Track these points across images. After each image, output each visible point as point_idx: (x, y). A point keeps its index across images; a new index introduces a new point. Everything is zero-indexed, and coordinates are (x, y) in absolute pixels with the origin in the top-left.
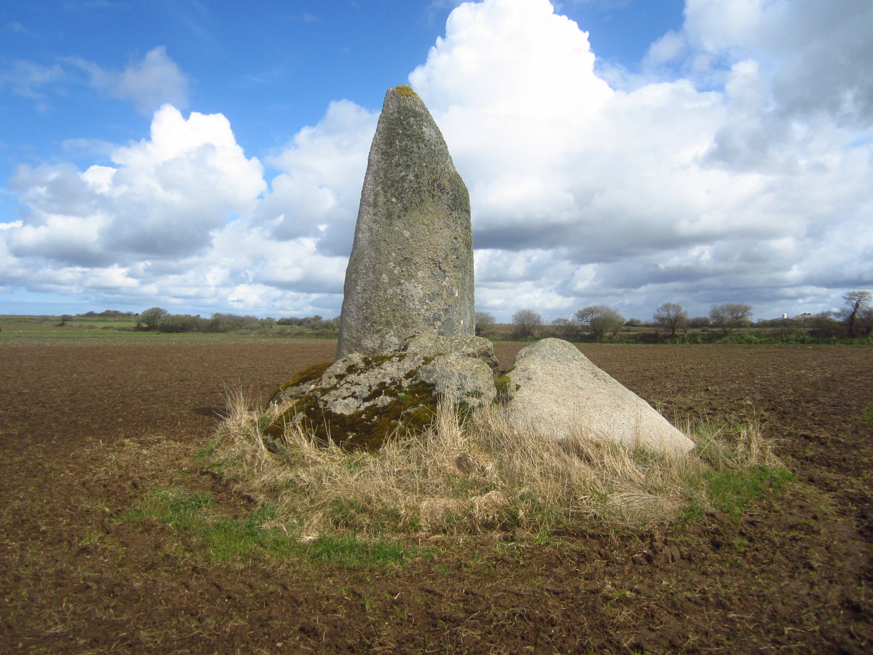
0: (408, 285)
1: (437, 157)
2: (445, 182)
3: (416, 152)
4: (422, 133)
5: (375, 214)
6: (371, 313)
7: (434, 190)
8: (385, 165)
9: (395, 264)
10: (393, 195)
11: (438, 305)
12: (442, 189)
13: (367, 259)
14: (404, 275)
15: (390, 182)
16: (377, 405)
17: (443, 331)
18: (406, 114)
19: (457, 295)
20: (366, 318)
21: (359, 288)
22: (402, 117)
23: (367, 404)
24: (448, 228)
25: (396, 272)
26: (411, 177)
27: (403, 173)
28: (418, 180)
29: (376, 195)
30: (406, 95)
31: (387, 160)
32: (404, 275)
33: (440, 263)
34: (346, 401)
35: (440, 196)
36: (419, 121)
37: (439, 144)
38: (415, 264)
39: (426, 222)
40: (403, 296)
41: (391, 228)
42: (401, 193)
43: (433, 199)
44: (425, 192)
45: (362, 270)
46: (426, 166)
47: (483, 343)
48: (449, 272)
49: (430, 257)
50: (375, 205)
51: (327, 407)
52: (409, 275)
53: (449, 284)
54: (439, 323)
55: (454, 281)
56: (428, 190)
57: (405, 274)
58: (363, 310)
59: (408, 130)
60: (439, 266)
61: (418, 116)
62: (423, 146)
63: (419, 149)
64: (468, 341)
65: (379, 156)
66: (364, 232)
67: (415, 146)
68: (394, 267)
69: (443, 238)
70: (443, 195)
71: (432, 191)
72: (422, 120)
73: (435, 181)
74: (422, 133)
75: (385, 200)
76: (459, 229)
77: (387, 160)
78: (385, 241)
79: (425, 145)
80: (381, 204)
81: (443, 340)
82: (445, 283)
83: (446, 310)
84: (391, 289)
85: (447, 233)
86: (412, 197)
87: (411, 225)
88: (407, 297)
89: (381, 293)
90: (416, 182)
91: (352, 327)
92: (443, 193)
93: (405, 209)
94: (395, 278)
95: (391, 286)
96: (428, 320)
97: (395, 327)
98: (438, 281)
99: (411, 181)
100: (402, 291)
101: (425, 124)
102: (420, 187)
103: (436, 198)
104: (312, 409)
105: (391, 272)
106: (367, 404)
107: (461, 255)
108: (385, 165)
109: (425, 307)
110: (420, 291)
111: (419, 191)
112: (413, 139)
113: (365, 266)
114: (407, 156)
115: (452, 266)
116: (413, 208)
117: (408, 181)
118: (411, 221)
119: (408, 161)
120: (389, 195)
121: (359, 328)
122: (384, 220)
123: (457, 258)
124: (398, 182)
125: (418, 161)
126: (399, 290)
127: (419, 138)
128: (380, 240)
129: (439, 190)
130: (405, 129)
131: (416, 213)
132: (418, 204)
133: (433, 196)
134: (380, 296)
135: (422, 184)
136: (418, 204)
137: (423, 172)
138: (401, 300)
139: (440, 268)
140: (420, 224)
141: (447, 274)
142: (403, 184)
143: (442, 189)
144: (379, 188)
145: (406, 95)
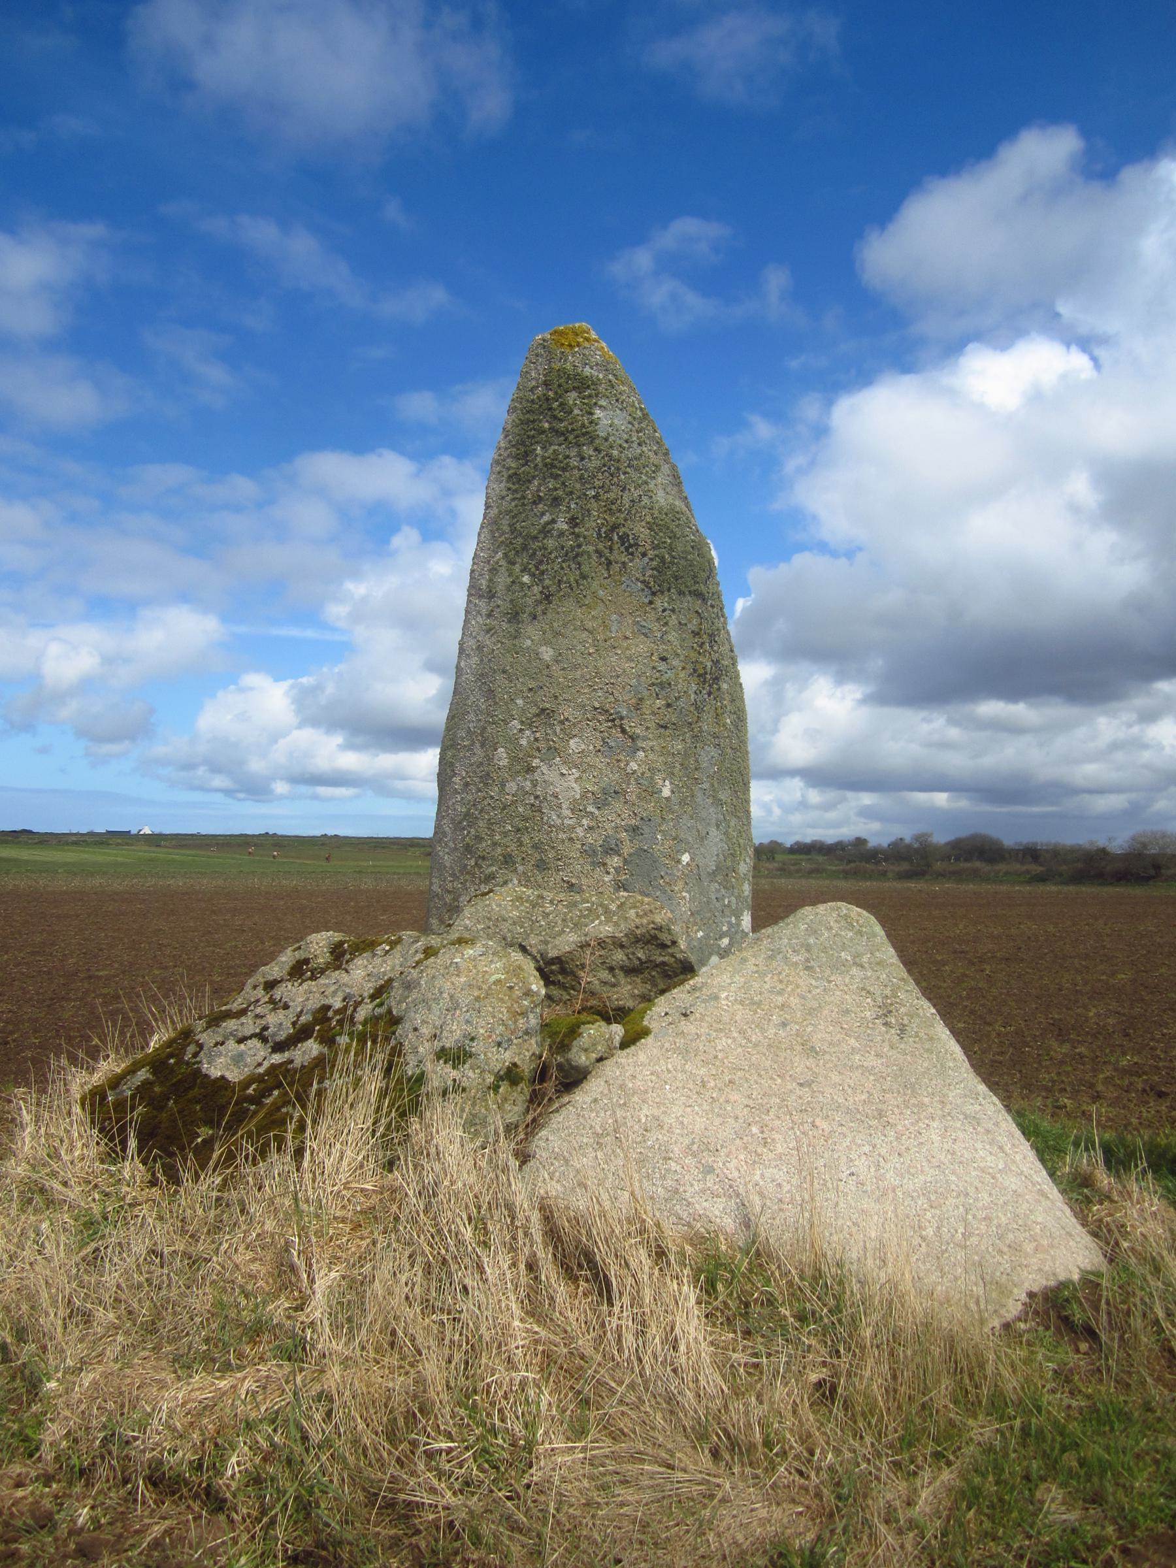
0: (546, 772)
1: (625, 473)
2: (640, 531)
3: (574, 467)
4: (591, 423)
5: (489, 615)
6: (477, 837)
7: (611, 549)
8: (513, 504)
9: (522, 723)
10: (524, 570)
11: (616, 817)
12: (631, 546)
13: (472, 717)
14: (538, 750)
15: (520, 540)
16: (292, 1062)
17: (626, 880)
18: (560, 386)
19: (666, 792)
20: (468, 849)
21: (456, 779)
22: (551, 394)
23: (277, 1058)
24: (646, 635)
25: (524, 742)
26: (562, 525)
27: (546, 518)
28: (577, 530)
29: (494, 571)
30: (570, 346)
31: (516, 491)
32: (538, 750)
33: (622, 718)
34: (242, 1046)
35: (624, 563)
36: (590, 396)
37: (635, 445)
38: (562, 722)
39: (589, 625)
40: (537, 797)
41: (516, 642)
42: (541, 562)
43: (608, 569)
44: (590, 557)
45: (463, 739)
46: (594, 497)
47: (645, 914)
48: (645, 739)
49: (597, 705)
50: (491, 595)
51: (198, 1059)
52: (549, 748)
53: (644, 768)
54: (615, 861)
55: (659, 761)
56: (597, 551)
57: (542, 745)
58: (464, 829)
59: (561, 421)
60: (621, 726)
61: (588, 387)
62: (591, 452)
63: (583, 459)
64: (613, 907)
65: (503, 485)
66: (468, 655)
67: (573, 452)
68: (521, 730)
69: (630, 659)
70: (631, 561)
71: (607, 551)
72: (597, 396)
73: (615, 527)
74: (591, 423)
75: (509, 580)
76: (673, 636)
77: (516, 491)
78: (504, 672)
79: (596, 449)
80: (500, 588)
81: (551, 902)
82: (634, 766)
83: (635, 830)
84: (514, 780)
85: (642, 647)
86: (562, 568)
87: (557, 634)
88: (545, 799)
89: (494, 792)
90: (573, 533)
91: (445, 867)
92: (632, 554)
93: (547, 597)
94: (521, 756)
95: (514, 775)
96: (590, 852)
97: (521, 868)
98: (618, 761)
99: (561, 534)
100: (535, 784)
101: (603, 402)
102: (579, 546)
103: (616, 567)
104: (172, 1061)
105: (514, 741)
106: (277, 1058)
107: (677, 699)
108: (513, 504)
109: (585, 822)
110: (574, 785)
111: (577, 555)
112: (571, 437)
113: (469, 731)
114: (556, 477)
115: (652, 725)
116: (562, 593)
117: (555, 533)
118: (555, 625)
119: (556, 489)
120: (517, 568)
121: (457, 869)
122: (505, 625)
123: (669, 705)
124: (535, 538)
125: (578, 486)
126: (528, 783)
127: (584, 434)
128: (495, 672)
129: (622, 549)
130: (555, 417)
131: (570, 604)
132: (574, 585)
133: (609, 563)
134: (492, 797)
135: (585, 537)
136: (574, 585)
137: (588, 511)
138: (533, 805)
139: (624, 731)
140: (575, 629)
141: (640, 744)
142: (545, 541)
143: (629, 545)
144: (500, 555)
145: (570, 346)
